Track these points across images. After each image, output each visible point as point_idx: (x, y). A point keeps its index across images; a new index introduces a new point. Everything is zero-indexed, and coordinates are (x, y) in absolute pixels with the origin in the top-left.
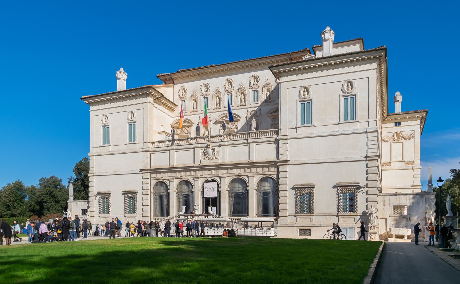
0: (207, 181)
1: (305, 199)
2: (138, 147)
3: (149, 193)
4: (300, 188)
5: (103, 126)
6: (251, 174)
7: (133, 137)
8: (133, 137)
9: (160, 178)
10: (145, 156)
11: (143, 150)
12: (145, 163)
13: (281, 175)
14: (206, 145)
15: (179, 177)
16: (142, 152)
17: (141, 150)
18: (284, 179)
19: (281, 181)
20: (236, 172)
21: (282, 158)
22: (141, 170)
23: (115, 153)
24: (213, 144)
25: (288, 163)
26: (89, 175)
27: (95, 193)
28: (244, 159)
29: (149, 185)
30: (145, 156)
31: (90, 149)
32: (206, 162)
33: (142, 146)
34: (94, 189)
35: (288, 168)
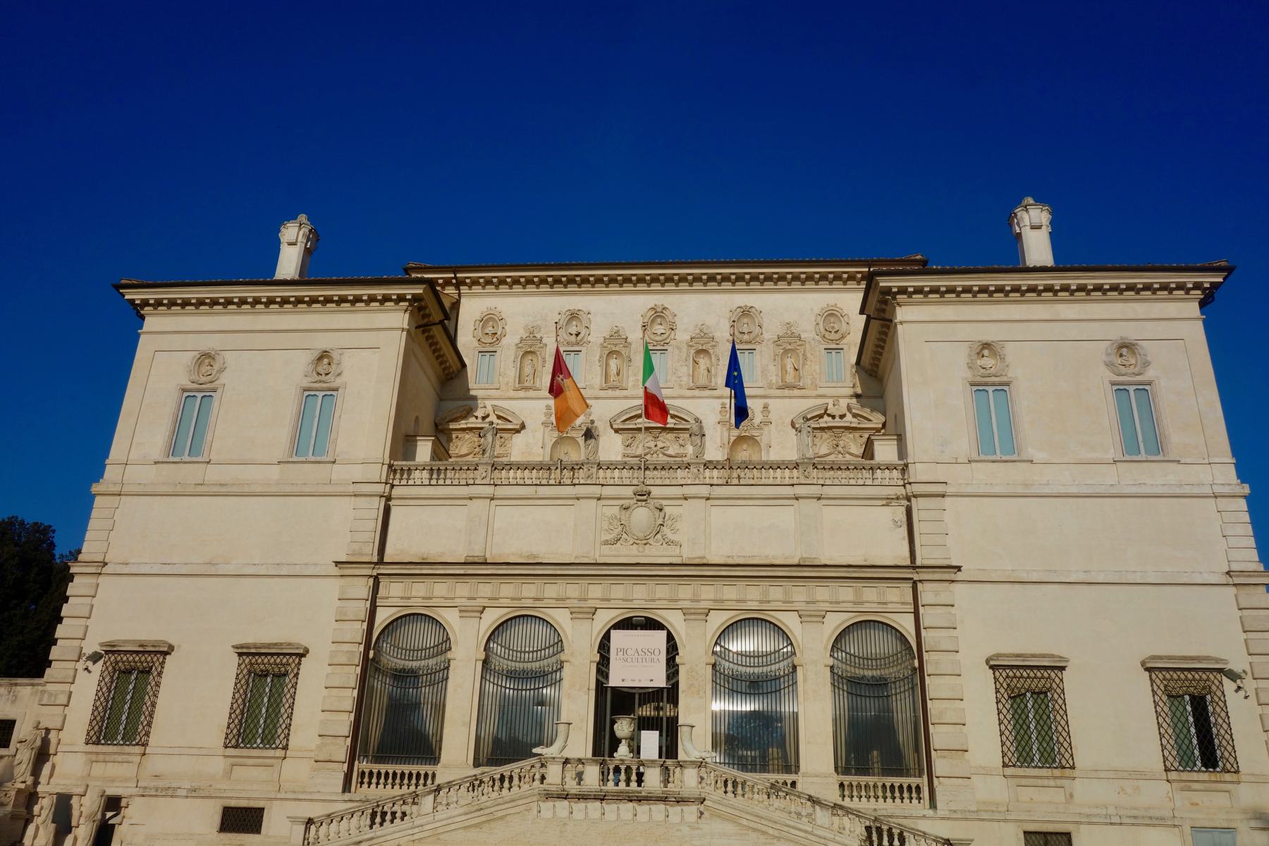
0: (626, 624)
4: (1011, 667)
6: (812, 607)
9: (420, 602)
23: (223, 490)
25: (960, 576)
27: (91, 647)
31: (105, 466)
32: (626, 552)
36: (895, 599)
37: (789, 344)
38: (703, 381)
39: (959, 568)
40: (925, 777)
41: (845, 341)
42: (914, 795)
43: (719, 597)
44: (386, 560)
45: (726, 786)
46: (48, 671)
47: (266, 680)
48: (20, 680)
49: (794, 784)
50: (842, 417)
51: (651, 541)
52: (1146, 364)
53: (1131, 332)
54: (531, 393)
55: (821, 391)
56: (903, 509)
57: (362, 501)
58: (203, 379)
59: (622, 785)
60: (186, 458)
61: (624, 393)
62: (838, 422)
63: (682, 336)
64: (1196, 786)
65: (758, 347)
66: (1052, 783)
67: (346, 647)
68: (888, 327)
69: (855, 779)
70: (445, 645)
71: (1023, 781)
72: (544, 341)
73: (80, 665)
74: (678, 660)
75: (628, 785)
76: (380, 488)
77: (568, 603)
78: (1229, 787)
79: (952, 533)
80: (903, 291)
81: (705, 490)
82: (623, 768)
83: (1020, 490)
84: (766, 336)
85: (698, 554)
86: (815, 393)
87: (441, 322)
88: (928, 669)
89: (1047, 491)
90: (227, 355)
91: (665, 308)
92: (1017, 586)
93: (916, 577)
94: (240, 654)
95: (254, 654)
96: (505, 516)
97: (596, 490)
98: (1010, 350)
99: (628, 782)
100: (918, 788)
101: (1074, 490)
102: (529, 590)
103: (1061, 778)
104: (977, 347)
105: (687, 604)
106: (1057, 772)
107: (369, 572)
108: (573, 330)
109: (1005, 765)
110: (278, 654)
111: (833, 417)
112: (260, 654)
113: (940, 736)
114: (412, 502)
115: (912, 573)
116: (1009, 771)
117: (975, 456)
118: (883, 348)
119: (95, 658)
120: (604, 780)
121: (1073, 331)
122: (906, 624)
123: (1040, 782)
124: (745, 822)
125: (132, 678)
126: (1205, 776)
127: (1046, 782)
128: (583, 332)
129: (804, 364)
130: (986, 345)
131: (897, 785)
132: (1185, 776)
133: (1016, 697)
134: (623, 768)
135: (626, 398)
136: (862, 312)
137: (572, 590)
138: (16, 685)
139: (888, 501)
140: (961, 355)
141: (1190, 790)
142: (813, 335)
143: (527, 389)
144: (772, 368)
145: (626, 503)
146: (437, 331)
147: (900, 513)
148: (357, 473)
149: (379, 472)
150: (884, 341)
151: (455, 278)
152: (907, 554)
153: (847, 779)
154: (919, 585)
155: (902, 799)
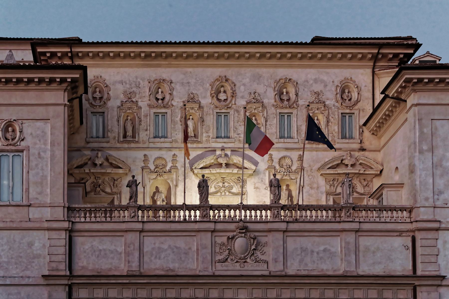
16: (48, 229)
25: (444, 283)
39: (444, 277)
44: (75, 274)
51: (248, 260)
57: (54, 234)
61: (200, 145)
65: (295, 111)
76: (66, 225)
84: (301, 102)
93: (417, 283)
114: (86, 234)
128: (168, 97)
148: (47, 213)
149: (60, 213)
151: (71, 52)
152: (411, 267)
154: (418, 289)
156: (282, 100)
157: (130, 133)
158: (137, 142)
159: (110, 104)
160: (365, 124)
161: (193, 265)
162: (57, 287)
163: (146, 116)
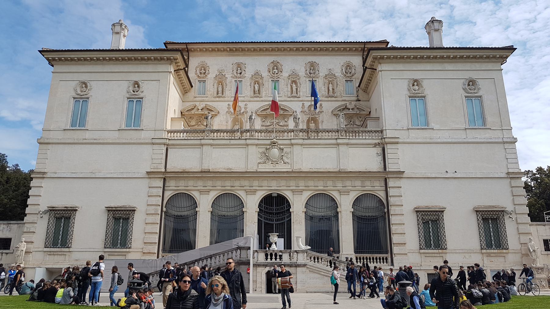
1: (431, 226)
2: (145, 136)
3: (159, 212)
5: (74, 98)
6: (344, 189)
7: (134, 119)
8: (134, 119)
10: (155, 152)
11: (154, 141)
12: (155, 161)
13: (391, 192)
14: (268, 142)
15: (219, 188)
17: (150, 141)
18: (397, 199)
19: (392, 200)
20: (320, 186)
21: (391, 167)
22: (148, 173)
24: (280, 142)
26: (32, 176)
28: (330, 166)
29: (160, 199)
30: (155, 152)
32: (268, 167)
33: (152, 134)
34: (40, 201)
35: (401, 183)
36: (378, 185)
37: (331, 78)
38: (294, 94)
40: (389, 254)
41: (353, 77)
42: (385, 261)
43: (307, 184)
45: (311, 258)
46: (25, 218)
47: (120, 221)
48: (12, 222)
49: (338, 258)
50: (352, 109)
52: (479, 89)
53: (474, 75)
54: (221, 99)
55: (344, 98)
56: (381, 148)
57: (156, 147)
58: (82, 94)
59: (274, 260)
60: (78, 128)
61: (261, 99)
62: (351, 112)
63: (285, 74)
64: (492, 255)
65: (317, 80)
66: (438, 255)
67: (153, 207)
68: (374, 72)
69: (362, 255)
70: (195, 204)
71: (428, 255)
72: (226, 76)
73: (39, 216)
74: (291, 210)
75: (271, 260)
77: (245, 188)
78: (505, 255)
79: (400, 158)
80: (382, 58)
81: (301, 141)
82: (274, 254)
83: (428, 141)
84: (321, 74)
85: (299, 168)
86: (341, 99)
87: (184, 68)
88: (391, 212)
89: (439, 141)
90: (92, 83)
91: (278, 62)
92: (426, 180)
94: (109, 211)
95: (114, 211)
96: (216, 153)
97: (256, 142)
98: (425, 83)
99: (271, 259)
100: (387, 259)
101: (450, 140)
102: (228, 183)
103: (442, 253)
104: (412, 82)
105: (294, 188)
106: (440, 251)
107: (162, 176)
108: (239, 71)
109: (421, 249)
110: (125, 210)
111: (349, 109)
112: (117, 211)
113: (395, 239)
115: (385, 176)
116: (422, 251)
117: (410, 127)
118: (371, 80)
119: (45, 212)
120: (267, 259)
121: (450, 75)
122: (381, 195)
123: (434, 255)
124: (323, 273)
125: (62, 221)
126: (496, 251)
127: (436, 255)
129: (337, 87)
130: (416, 81)
131: (378, 257)
132: (488, 251)
133: (426, 223)
134: (274, 254)
135: (262, 101)
136: (363, 66)
137: (246, 183)
138: (10, 224)
139: (375, 145)
140: (404, 85)
141: (490, 256)
142: (340, 74)
143: (219, 97)
144: (323, 88)
145: (268, 147)
146: (182, 73)
147: (379, 150)
150: (372, 78)
153: (359, 255)
155: (380, 262)
156: (310, 73)
157: (220, 92)
158: (224, 97)
159: (209, 76)
160: (359, 86)
161: (238, 166)
162: (156, 179)
163: (231, 82)
